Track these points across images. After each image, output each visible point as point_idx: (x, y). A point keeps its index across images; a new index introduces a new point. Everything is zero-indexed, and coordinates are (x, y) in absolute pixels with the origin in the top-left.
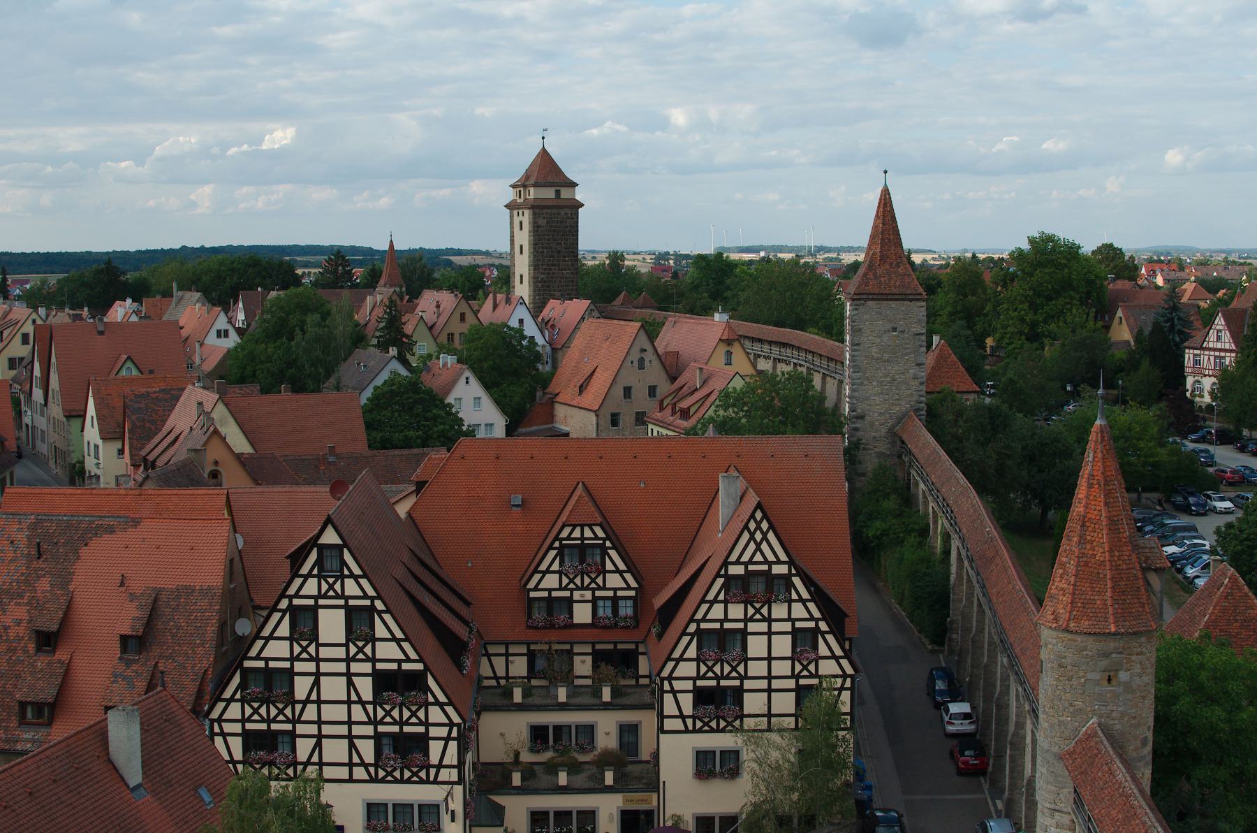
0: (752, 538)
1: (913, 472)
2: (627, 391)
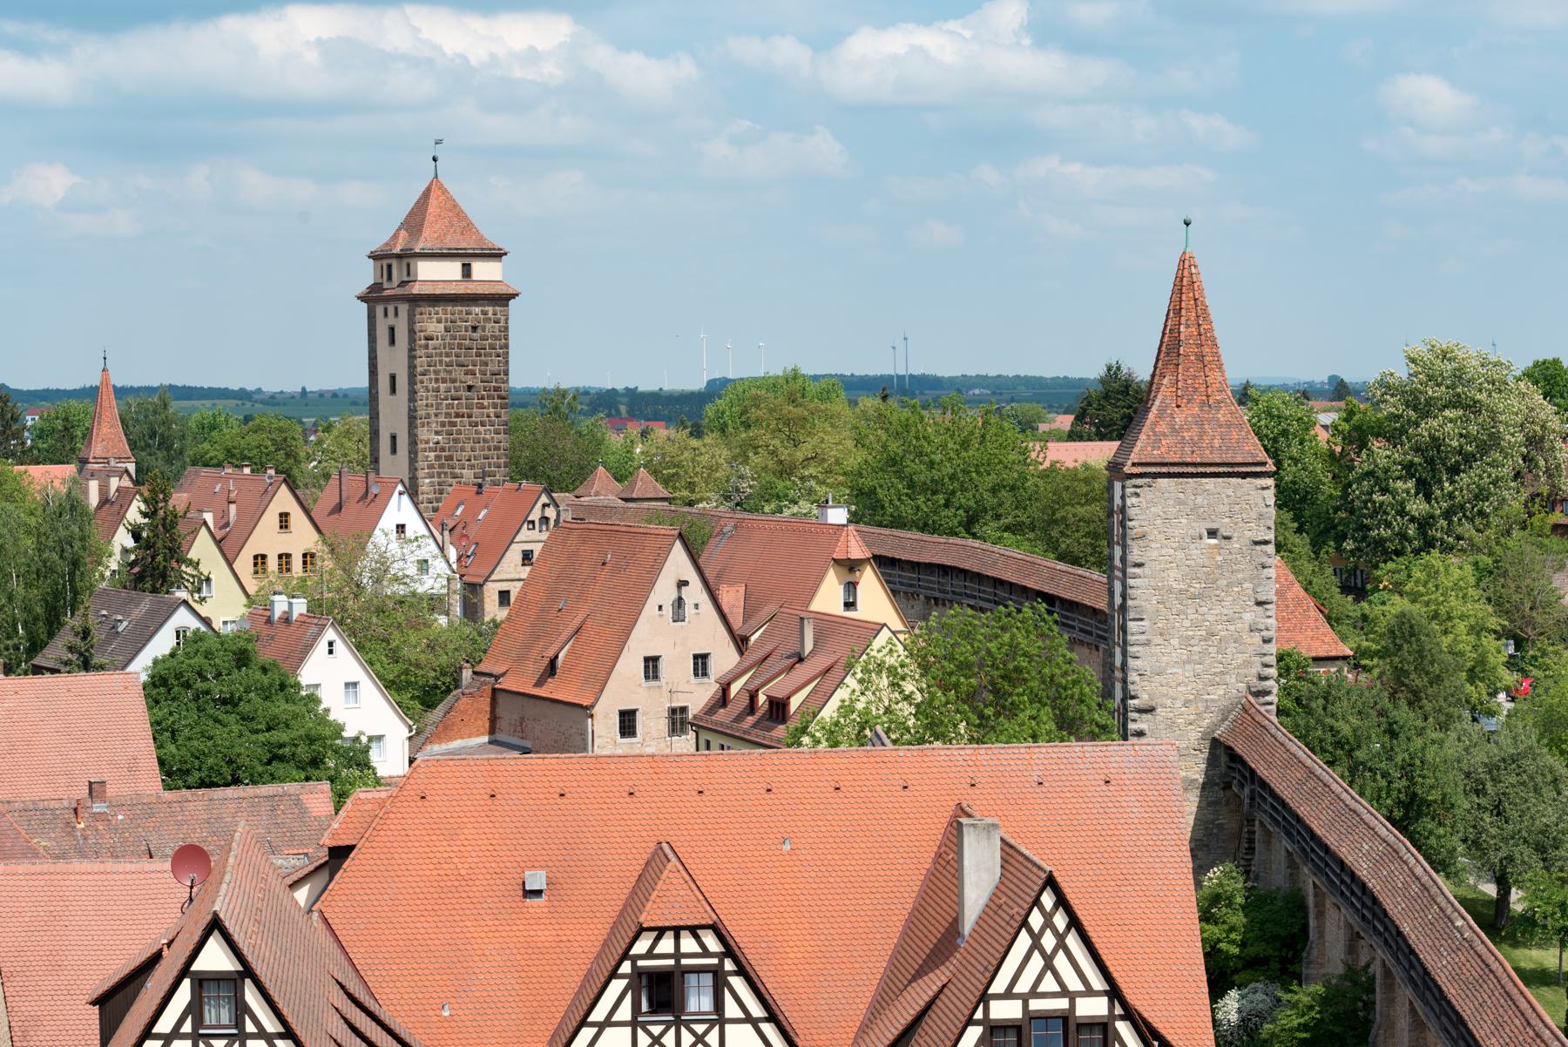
0: (1036, 944)
1: (1259, 816)
2: (652, 665)
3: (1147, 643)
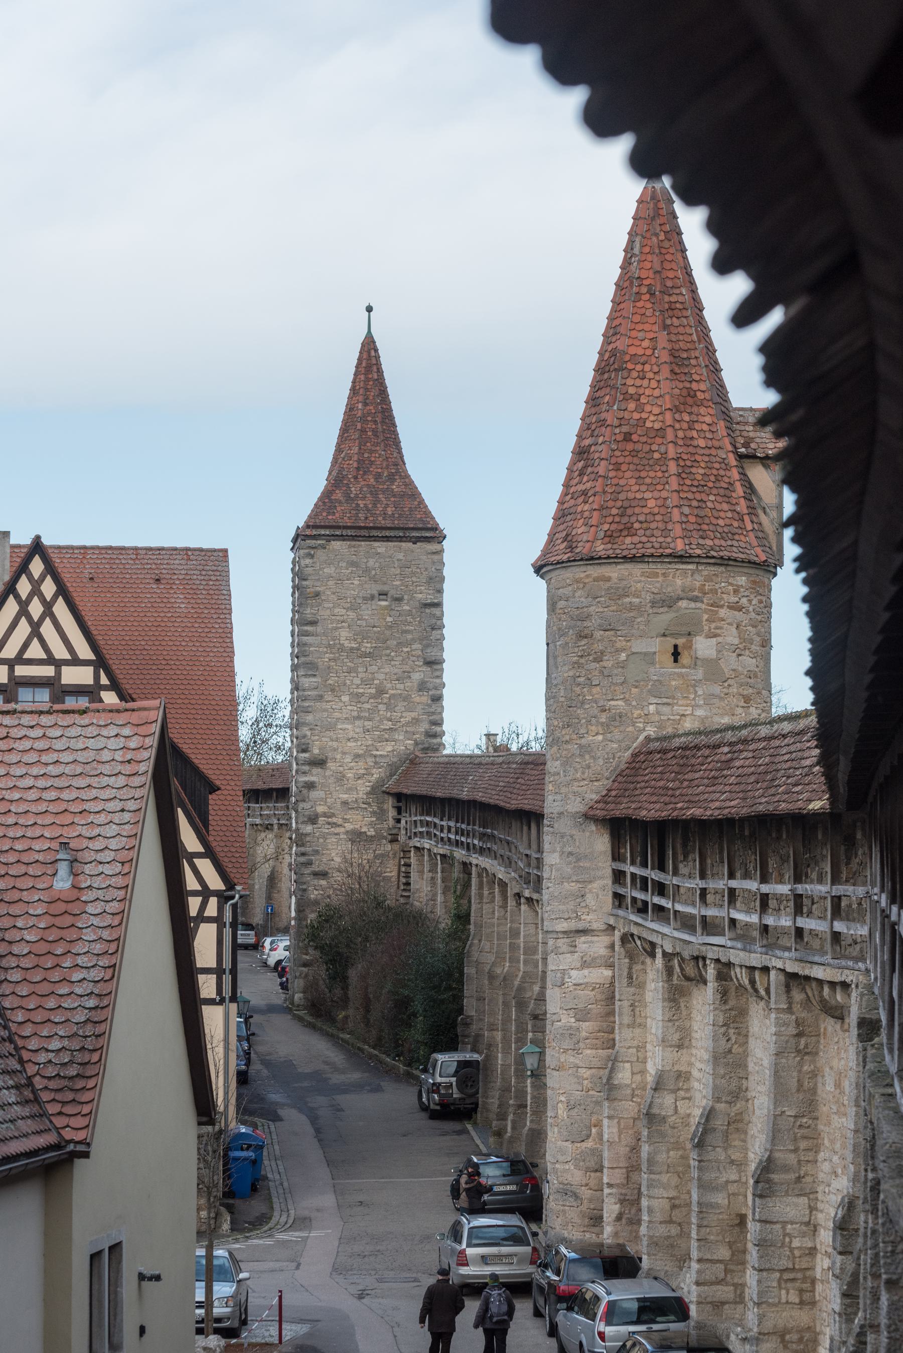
0: (23, 611)
3: (320, 698)
